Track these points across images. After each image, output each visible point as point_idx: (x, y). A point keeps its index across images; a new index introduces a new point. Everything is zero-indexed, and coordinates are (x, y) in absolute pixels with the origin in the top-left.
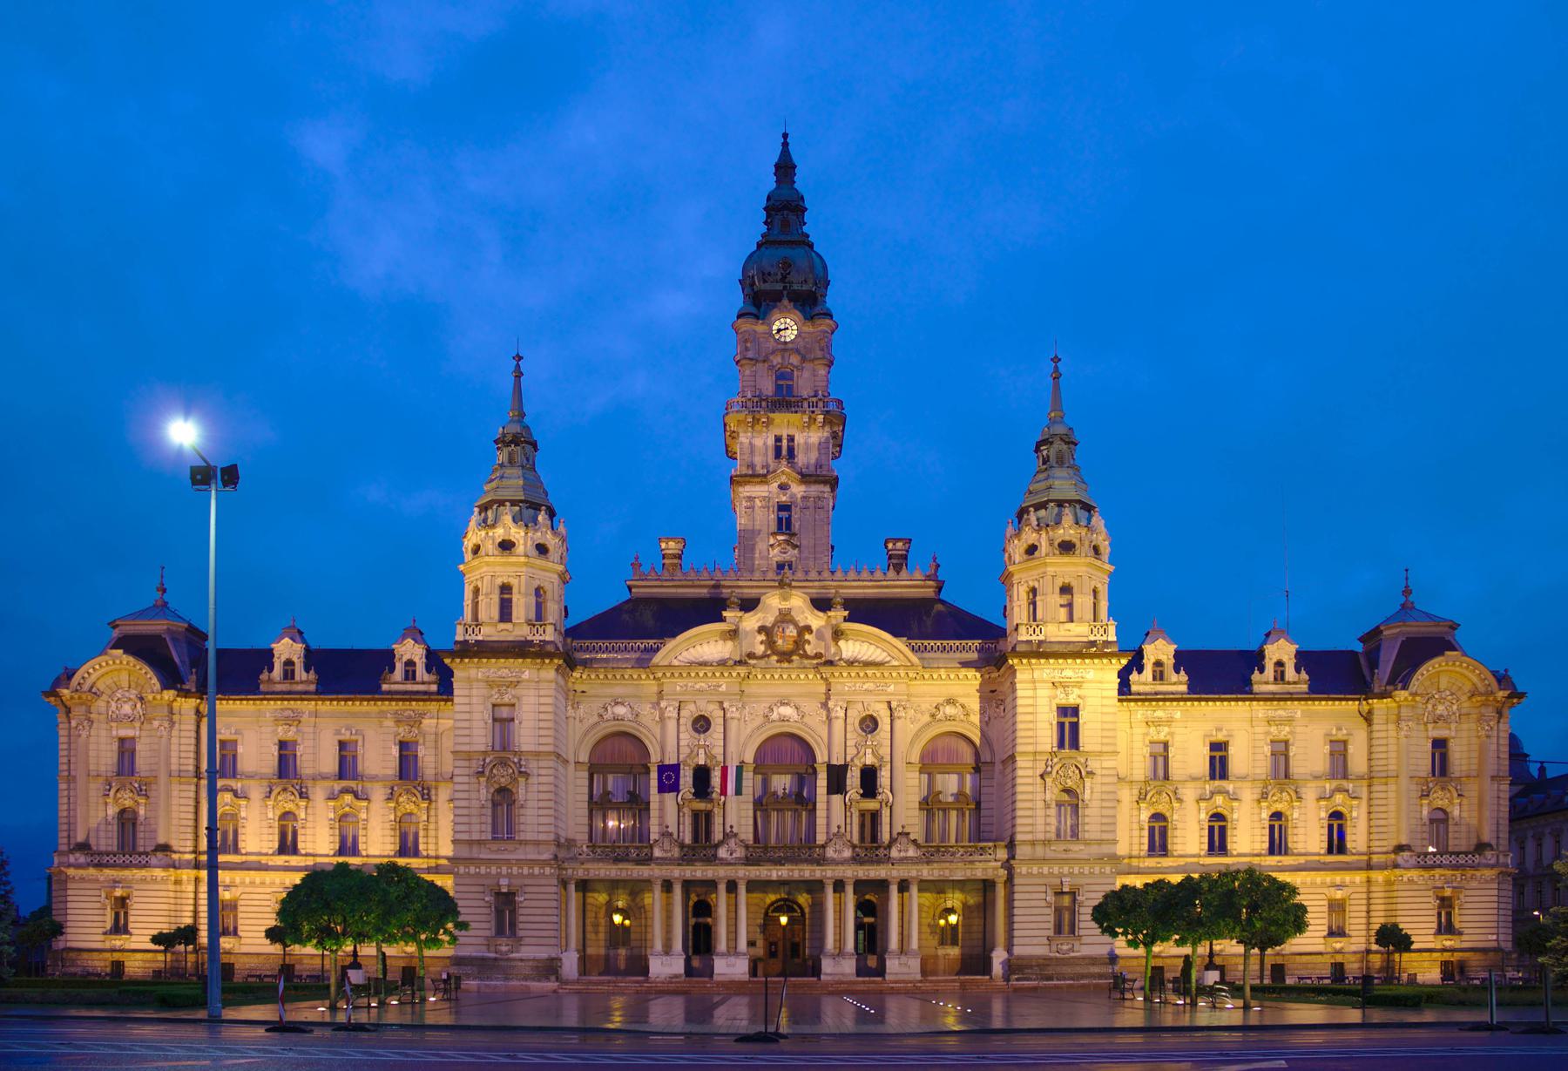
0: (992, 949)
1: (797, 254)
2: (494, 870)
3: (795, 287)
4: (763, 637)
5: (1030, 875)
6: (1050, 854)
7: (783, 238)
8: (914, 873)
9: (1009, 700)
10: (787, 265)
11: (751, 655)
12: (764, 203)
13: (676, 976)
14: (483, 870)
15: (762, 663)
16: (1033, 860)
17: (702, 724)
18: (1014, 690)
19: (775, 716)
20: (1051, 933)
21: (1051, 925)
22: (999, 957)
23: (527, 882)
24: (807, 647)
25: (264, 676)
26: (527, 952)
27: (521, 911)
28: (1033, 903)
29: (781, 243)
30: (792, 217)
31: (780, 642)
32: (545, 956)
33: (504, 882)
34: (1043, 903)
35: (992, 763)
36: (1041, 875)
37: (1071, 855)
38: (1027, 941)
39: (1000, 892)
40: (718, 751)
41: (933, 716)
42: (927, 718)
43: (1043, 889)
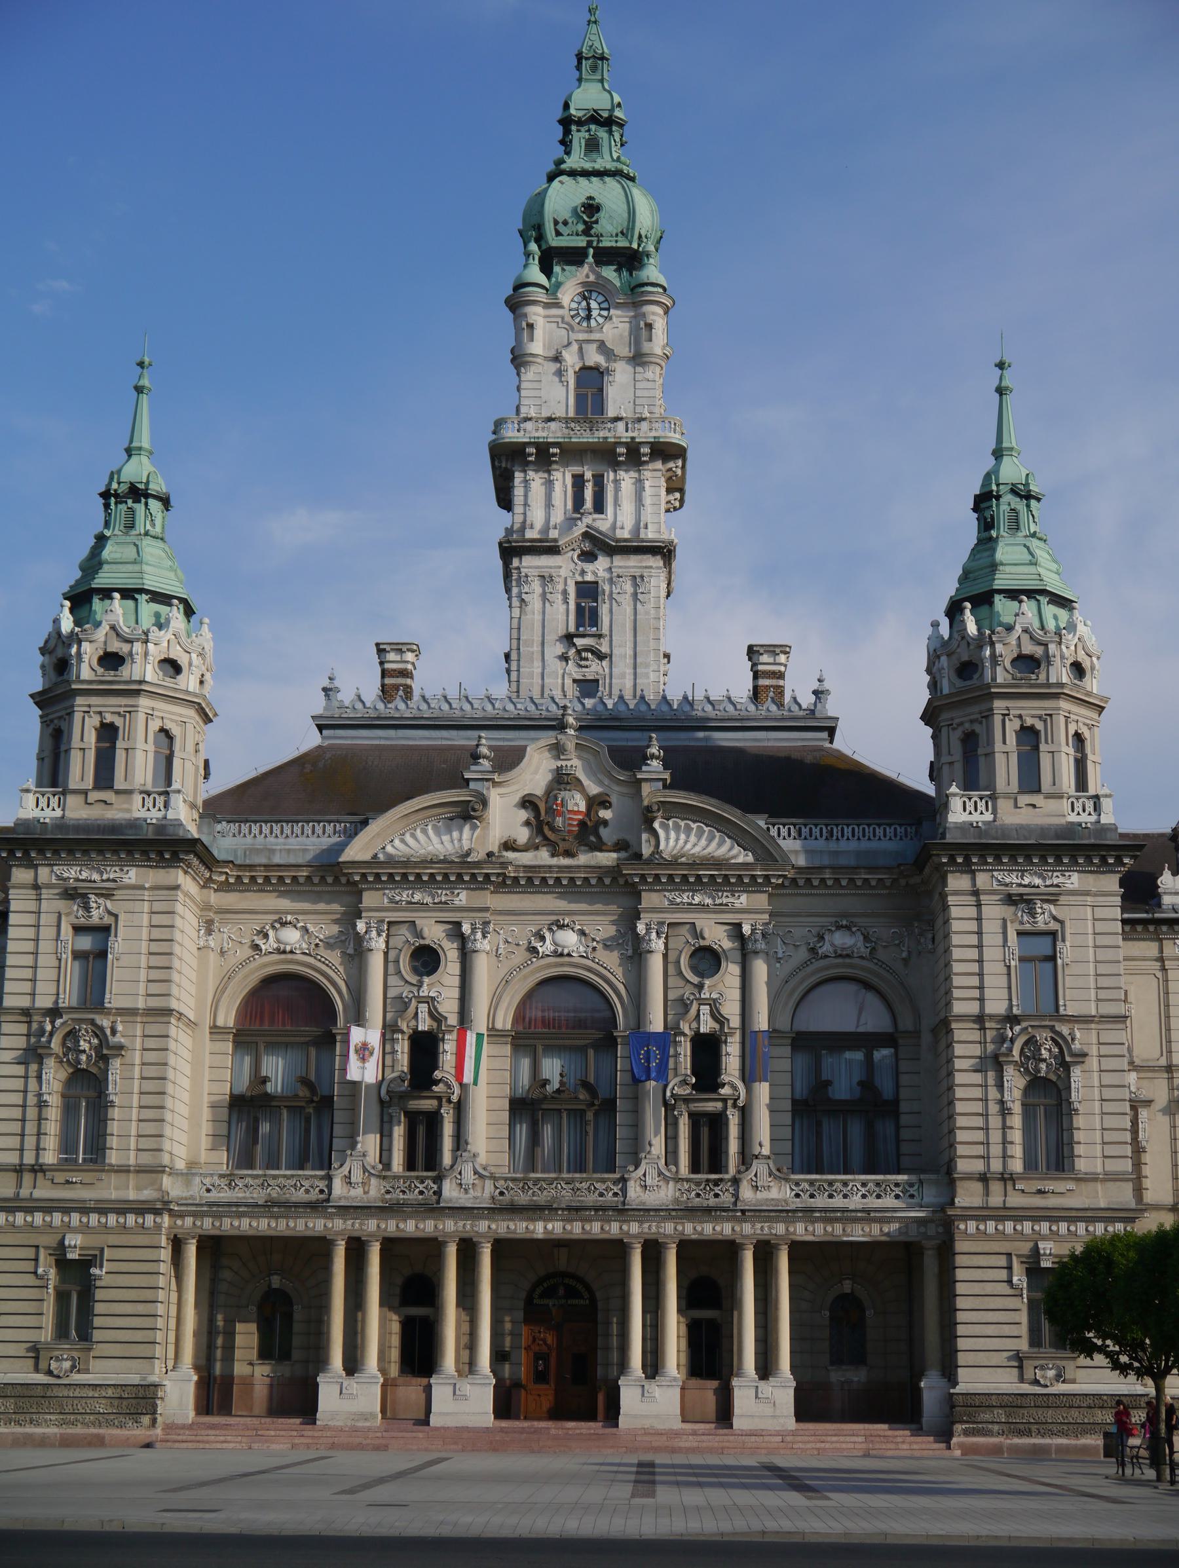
0: (920, 1375)
1: (608, 193)
2: (57, 1218)
3: (606, 243)
5: (982, 1235)
6: (1015, 1200)
7: (588, 166)
9: (940, 922)
10: (591, 208)
11: (508, 846)
12: (559, 114)
14: (38, 1219)
15: (527, 858)
16: (983, 1214)
17: (426, 959)
19: (547, 947)
20: (1023, 1345)
21: (1024, 1330)
23: (113, 1239)
24: (604, 832)
26: (105, 1371)
27: (99, 1294)
28: (989, 1288)
29: (586, 174)
30: (602, 133)
31: (559, 821)
32: (135, 1379)
33: (72, 1240)
34: (1004, 1289)
35: (916, 1034)
36: (1001, 1235)
37: (1052, 1202)
38: (981, 1358)
39: (930, 1263)
40: (449, 1007)
41: (813, 950)
42: (803, 954)
43: (1002, 1261)
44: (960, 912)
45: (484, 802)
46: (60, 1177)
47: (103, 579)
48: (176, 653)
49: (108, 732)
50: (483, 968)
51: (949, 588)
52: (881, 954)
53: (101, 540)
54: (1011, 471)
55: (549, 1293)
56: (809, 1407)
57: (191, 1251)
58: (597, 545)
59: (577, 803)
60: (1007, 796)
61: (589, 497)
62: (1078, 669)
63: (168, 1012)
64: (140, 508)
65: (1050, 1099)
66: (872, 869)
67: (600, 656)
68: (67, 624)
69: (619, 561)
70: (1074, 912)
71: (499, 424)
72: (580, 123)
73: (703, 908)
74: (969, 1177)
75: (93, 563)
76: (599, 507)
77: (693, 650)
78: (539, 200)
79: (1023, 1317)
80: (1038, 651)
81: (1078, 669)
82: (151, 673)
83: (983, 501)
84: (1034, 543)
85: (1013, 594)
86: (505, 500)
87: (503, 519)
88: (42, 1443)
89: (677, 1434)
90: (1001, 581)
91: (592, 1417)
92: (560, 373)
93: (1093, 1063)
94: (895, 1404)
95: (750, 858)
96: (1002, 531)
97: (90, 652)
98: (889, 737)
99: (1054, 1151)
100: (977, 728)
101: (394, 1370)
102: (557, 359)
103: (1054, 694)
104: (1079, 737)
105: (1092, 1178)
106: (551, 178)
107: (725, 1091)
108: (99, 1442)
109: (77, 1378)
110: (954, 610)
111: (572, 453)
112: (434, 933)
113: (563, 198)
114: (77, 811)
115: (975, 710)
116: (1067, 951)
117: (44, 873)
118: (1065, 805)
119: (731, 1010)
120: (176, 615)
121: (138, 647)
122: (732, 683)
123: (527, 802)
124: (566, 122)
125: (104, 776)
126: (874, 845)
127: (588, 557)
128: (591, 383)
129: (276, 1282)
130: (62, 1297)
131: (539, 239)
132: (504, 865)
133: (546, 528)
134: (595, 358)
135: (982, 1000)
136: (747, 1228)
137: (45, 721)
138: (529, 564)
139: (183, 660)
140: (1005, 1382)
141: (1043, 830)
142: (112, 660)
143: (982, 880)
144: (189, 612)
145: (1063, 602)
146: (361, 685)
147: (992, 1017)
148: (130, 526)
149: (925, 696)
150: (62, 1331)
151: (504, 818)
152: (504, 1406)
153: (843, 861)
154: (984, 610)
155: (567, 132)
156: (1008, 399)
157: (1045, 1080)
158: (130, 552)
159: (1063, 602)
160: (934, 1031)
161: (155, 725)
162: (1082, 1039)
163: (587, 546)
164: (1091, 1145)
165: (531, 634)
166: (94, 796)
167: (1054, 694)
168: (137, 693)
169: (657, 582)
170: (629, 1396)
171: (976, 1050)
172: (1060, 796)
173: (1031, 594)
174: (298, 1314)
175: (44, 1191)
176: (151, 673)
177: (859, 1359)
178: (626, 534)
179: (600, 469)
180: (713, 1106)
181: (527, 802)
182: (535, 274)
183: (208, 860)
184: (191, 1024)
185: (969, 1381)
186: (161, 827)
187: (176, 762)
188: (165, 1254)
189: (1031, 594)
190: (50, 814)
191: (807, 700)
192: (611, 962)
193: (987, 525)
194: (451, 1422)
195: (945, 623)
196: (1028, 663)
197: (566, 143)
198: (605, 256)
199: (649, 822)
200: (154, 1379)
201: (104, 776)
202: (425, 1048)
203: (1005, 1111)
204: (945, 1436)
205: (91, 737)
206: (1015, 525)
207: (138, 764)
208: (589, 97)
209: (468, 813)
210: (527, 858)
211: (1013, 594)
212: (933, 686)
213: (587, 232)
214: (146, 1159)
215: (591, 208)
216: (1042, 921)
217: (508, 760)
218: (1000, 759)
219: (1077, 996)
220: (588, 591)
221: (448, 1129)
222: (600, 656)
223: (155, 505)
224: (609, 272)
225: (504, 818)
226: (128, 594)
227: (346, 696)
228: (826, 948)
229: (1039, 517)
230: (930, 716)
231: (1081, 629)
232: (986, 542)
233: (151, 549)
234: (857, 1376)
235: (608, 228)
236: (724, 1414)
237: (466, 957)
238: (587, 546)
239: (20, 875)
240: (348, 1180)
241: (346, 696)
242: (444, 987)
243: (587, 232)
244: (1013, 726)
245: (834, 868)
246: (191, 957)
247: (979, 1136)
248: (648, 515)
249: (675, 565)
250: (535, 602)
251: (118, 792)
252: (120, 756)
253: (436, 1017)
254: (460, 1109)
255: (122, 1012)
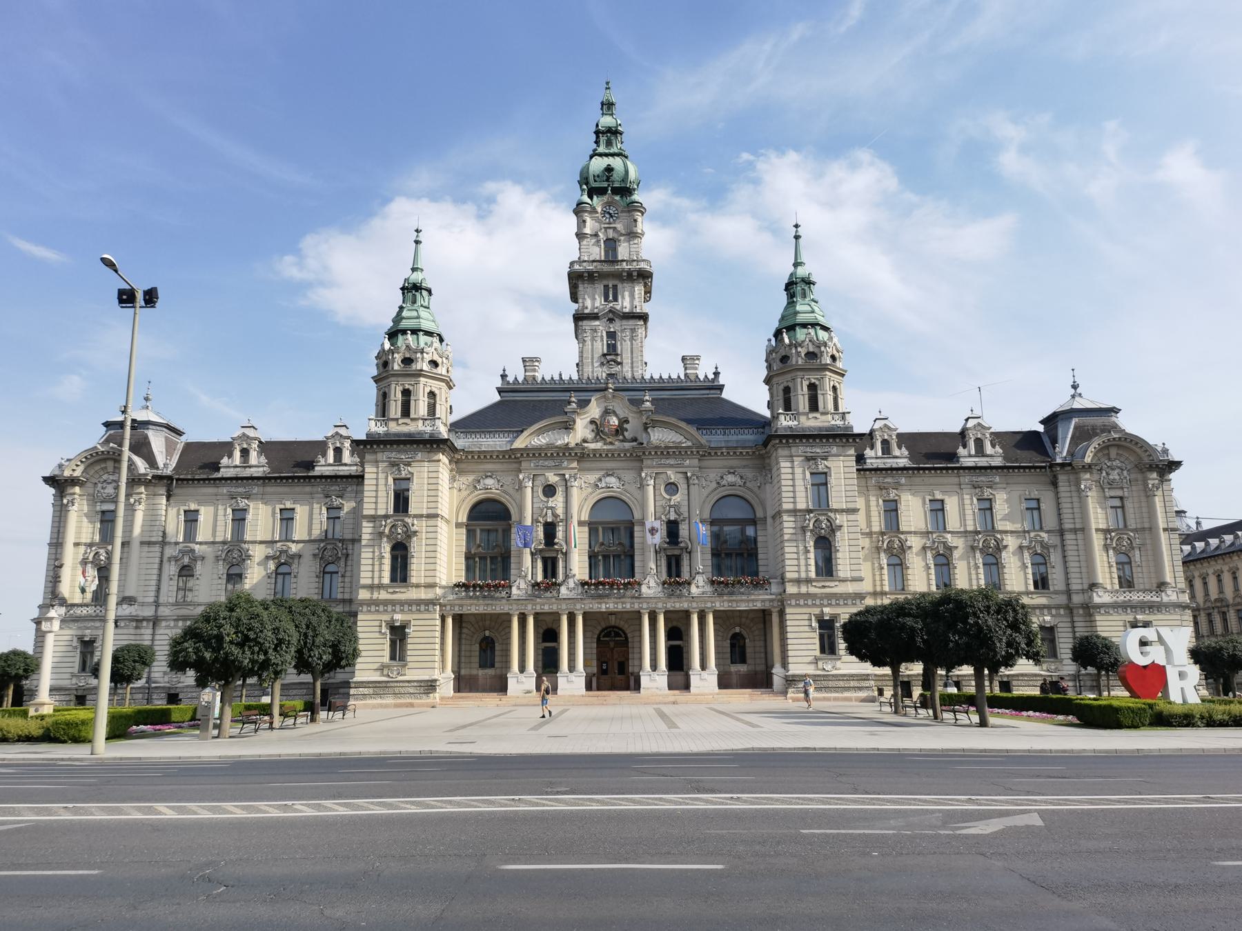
0: (772, 666)
1: (616, 163)
4: (594, 427)
6: (812, 590)
8: (709, 605)
9: (774, 469)
10: (609, 169)
11: (585, 441)
12: (594, 129)
13: (529, 692)
17: (550, 491)
18: (778, 463)
20: (817, 653)
21: (817, 647)
22: (777, 671)
25: (225, 461)
26: (412, 674)
27: (409, 641)
28: (802, 629)
29: (607, 155)
32: (427, 678)
34: (807, 629)
39: (775, 618)
40: (560, 511)
42: (714, 485)
43: (806, 617)
44: (785, 465)
45: (574, 422)
46: (391, 590)
47: (404, 324)
48: (436, 358)
49: (406, 393)
50: (575, 492)
51: (776, 325)
52: (748, 484)
53: (401, 308)
54: (801, 272)
55: (608, 635)
56: (724, 683)
57: (449, 621)
58: (614, 315)
59: (614, 421)
60: (804, 414)
61: (611, 294)
62: (833, 358)
63: (436, 516)
64: (418, 294)
65: (825, 544)
66: (744, 448)
67: (619, 364)
68: (387, 346)
69: (624, 322)
70: (835, 464)
71: (572, 264)
72: (603, 133)
73: (671, 466)
74: (791, 581)
75: (398, 318)
76: (615, 299)
77: (659, 356)
78: (587, 168)
79: (817, 641)
80: (816, 350)
81: (833, 358)
82: (426, 367)
83: (790, 286)
84: (813, 304)
85: (804, 326)
86: (574, 298)
87: (575, 306)
88: (386, 706)
89: (667, 696)
90: (801, 318)
91: (627, 688)
92: (598, 241)
93: (845, 529)
94: (760, 680)
95: (689, 444)
96: (799, 299)
97: (398, 357)
98: (748, 391)
99: (827, 568)
100: (790, 385)
101: (540, 671)
102: (596, 235)
103: (825, 368)
104: (834, 388)
105: (844, 580)
106: (591, 157)
107: (682, 545)
108: (412, 705)
109: (400, 678)
110: (778, 334)
111: (603, 276)
112: (552, 478)
113: (598, 164)
114: (394, 428)
115: (788, 377)
116: (833, 480)
117: (380, 456)
118: (830, 417)
119: (684, 510)
120: (436, 340)
121: (419, 355)
122: (676, 371)
123: (592, 422)
124: (597, 133)
125: (406, 412)
126: (744, 437)
127: (611, 320)
128: (611, 245)
129: (487, 633)
130: (393, 643)
131: (587, 184)
132: (583, 449)
133: (594, 308)
134: (611, 234)
135: (794, 503)
136: (694, 605)
137: (379, 390)
138: (586, 324)
139: (439, 361)
140: (810, 670)
141: (820, 429)
142: (407, 361)
143: (794, 450)
144: (441, 340)
145: (825, 329)
146: (517, 373)
147: (800, 511)
148: (414, 302)
149: (765, 373)
150: (393, 658)
151: (582, 429)
152: (589, 687)
153: (730, 445)
154: (792, 333)
155: (598, 137)
156: (801, 240)
157: (824, 538)
158: (415, 314)
159: (825, 329)
160: (774, 517)
161: (427, 390)
162: (840, 519)
163: (611, 315)
164: (843, 566)
165: (587, 354)
166: (401, 421)
167: (825, 368)
168: (420, 375)
169: (641, 331)
170: (644, 681)
171: (792, 525)
172: (827, 413)
173: (814, 325)
174: (498, 647)
175: (383, 595)
176: (426, 367)
177: (743, 660)
178: (627, 310)
179: (615, 282)
180: (677, 552)
181: (592, 422)
182: (586, 198)
183: (454, 449)
184: (447, 521)
185: (794, 669)
186: (431, 435)
187: (438, 406)
188: (438, 622)
189: (814, 325)
190: (381, 430)
191: (711, 376)
192: (633, 488)
193: (791, 297)
194: (568, 693)
195: (773, 340)
196: (811, 355)
197: (597, 142)
198: (616, 191)
199: (646, 429)
200: (435, 677)
201: (406, 412)
202: (550, 530)
203: (807, 551)
204: (785, 693)
205: (399, 395)
206: (804, 296)
207: (420, 407)
208: (607, 121)
209: (568, 427)
210: (592, 446)
211: (804, 326)
212: (769, 367)
213: (607, 180)
214: (429, 580)
215: (609, 169)
216: (821, 468)
217: (584, 404)
218: (801, 398)
219: (837, 499)
220: (611, 335)
221: (561, 564)
222: (619, 364)
223: (425, 293)
224: (617, 198)
225: (582, 429)
226: (415, 332)
227: (510, 379)
228: (724, 482)
229: (816, 292)
230: (768, 381)
231: (835, 340)
232: (791, 302)
233: (423, 312)
234: (743, 668)
235: (617, 176)
236: (687, 687)
237: (567, 489)
238: (611, 315)
239: (368, 457)
240: (519, 588)
241: (510, 379)
242: (558, 501)
243: (607, 180)
244: (805, 383)
245: (727, 448)
246: (443, 493)
247: (795, 562)
248: (636, 303)
249: (649, 324)
250: (588, 339)
251: (412, 420)
252: (412, 403)
253: (555, 515)
254: (566, 554)
255: (415, 516)
